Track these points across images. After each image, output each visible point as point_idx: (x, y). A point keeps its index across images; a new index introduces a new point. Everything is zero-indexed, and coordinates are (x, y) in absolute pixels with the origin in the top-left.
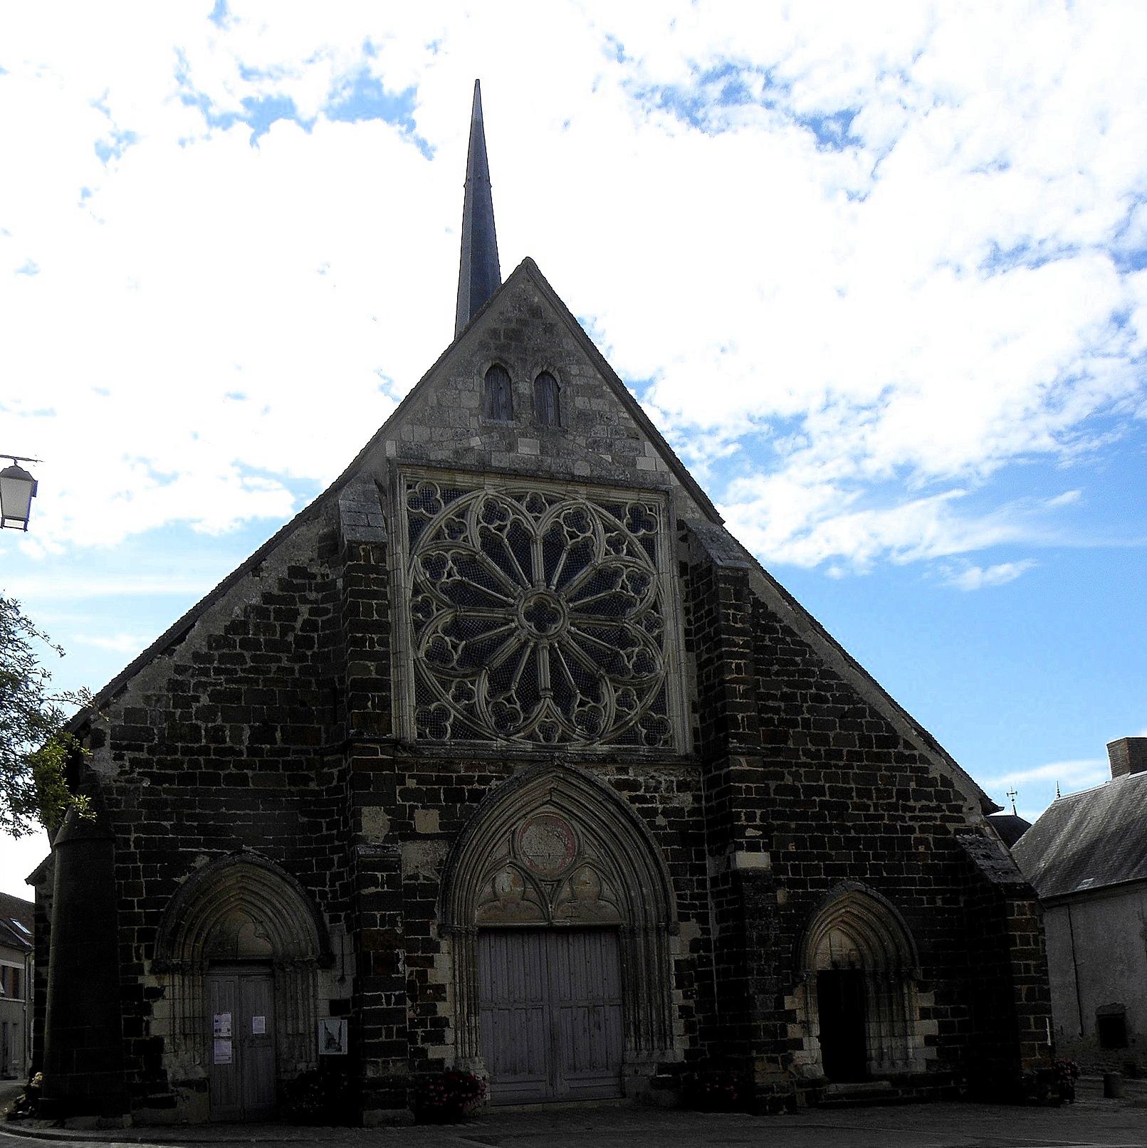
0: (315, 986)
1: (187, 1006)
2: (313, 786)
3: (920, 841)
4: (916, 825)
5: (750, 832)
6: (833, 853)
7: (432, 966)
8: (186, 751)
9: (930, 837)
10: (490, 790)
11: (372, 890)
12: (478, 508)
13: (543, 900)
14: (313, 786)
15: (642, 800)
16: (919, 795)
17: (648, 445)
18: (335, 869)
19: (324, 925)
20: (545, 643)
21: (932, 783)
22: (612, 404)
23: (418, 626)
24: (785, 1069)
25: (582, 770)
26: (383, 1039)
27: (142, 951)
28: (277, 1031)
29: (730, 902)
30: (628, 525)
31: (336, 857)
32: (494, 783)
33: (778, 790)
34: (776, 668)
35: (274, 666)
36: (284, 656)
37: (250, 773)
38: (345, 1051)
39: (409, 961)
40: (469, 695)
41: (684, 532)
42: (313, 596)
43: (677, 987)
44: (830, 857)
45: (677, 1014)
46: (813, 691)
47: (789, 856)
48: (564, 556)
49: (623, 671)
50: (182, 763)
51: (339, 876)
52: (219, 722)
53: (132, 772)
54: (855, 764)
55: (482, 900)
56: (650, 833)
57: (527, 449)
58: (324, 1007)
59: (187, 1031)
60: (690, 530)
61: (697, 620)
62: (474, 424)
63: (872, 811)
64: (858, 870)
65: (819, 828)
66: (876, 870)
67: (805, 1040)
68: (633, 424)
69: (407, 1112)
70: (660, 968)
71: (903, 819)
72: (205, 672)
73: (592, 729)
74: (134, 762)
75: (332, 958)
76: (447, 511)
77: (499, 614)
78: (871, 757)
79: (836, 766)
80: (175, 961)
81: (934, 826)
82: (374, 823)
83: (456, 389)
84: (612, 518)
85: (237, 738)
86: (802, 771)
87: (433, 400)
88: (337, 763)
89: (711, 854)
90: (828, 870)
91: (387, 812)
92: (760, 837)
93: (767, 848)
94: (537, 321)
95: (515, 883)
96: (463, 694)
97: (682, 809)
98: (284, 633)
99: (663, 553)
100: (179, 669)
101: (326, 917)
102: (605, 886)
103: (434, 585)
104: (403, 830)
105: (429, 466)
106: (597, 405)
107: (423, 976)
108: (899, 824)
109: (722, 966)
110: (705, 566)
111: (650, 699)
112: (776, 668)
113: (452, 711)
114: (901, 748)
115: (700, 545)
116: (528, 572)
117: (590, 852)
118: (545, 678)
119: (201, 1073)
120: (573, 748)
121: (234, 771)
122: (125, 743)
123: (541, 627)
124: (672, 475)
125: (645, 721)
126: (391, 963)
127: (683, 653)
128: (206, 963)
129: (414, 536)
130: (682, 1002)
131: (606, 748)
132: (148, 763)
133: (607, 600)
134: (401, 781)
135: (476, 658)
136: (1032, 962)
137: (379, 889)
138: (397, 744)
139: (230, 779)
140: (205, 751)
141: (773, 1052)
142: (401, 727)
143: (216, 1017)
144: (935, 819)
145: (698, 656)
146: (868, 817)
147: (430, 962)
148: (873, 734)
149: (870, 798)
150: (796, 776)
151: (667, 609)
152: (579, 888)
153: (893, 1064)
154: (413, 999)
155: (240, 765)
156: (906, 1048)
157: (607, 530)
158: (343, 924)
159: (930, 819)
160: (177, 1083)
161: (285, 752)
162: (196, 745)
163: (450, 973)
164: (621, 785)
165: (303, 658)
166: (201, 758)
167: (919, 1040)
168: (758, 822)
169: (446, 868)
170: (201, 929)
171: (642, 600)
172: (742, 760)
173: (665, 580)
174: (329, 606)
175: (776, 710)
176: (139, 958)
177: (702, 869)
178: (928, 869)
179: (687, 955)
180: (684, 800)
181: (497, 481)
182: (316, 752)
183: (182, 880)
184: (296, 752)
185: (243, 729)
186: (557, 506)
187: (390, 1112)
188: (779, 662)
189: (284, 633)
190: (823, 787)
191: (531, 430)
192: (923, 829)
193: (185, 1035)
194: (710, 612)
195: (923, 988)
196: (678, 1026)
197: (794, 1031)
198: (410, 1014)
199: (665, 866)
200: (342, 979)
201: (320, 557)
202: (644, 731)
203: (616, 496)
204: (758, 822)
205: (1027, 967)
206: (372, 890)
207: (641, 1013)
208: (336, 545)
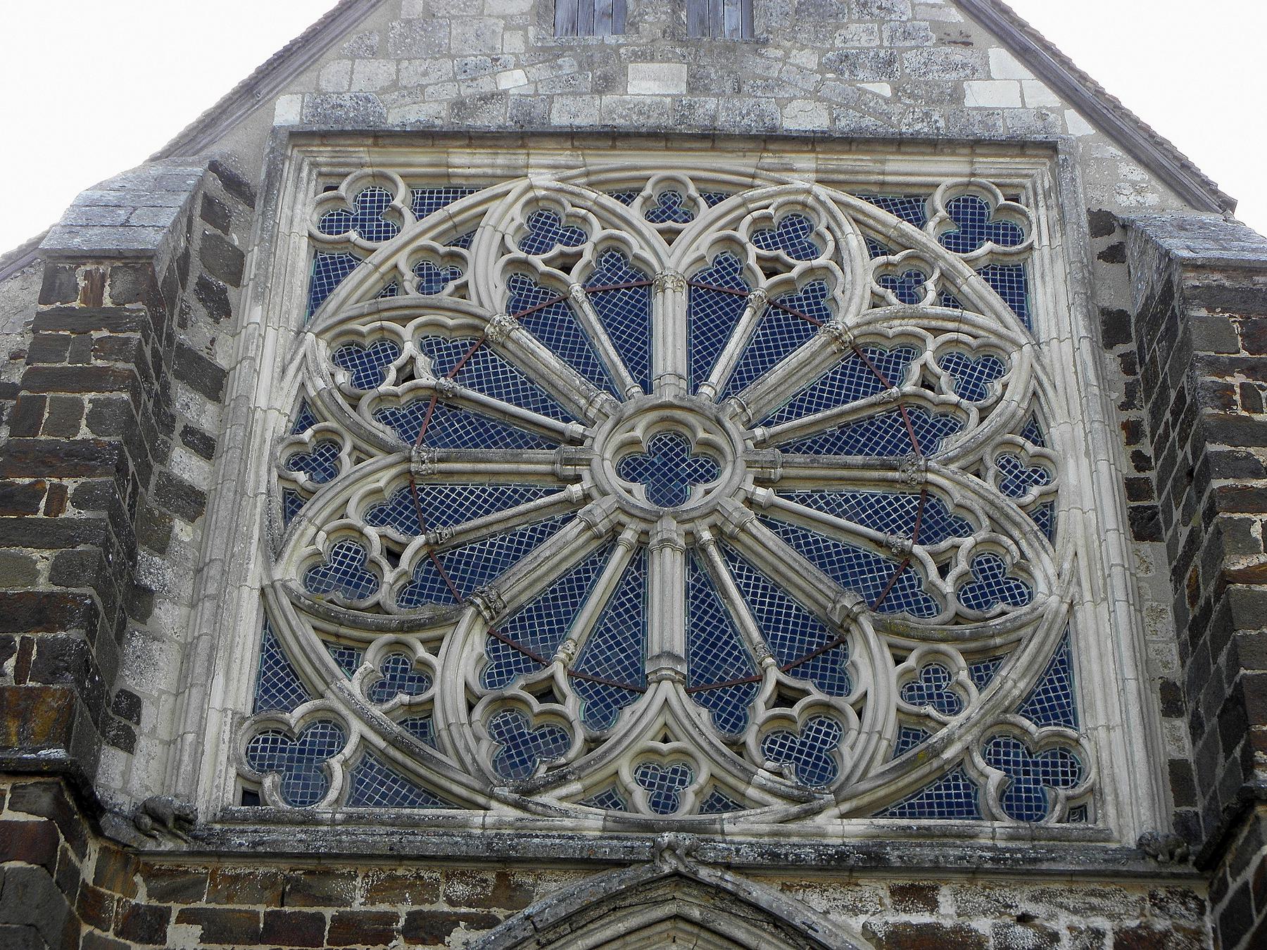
12: (504, 218)
17: (1000, 57)
25: (762, 893)
40: (423, 677)
41: (1114, 239)
49: (926, 604)
57: (652, 86)
62: (514, 43)
73: (811, 759)
77: (538, 461)
96: (406, 675)
103: (354, 402)
105: (380, 136)
111: (1014, 679)
113: (357, 727)
116: (638, 357)
118: (668, 624)
124: (1072, 115)
125: (999, 747)
131: (858, 826)
133: (873, 414)
135: (449, 580)
157: (875, 249)
171: (984, 413)
173: (1056, 352)
181: (564, 157)
191: (665, 45)
202: (996, 775)
203: (903, 169)
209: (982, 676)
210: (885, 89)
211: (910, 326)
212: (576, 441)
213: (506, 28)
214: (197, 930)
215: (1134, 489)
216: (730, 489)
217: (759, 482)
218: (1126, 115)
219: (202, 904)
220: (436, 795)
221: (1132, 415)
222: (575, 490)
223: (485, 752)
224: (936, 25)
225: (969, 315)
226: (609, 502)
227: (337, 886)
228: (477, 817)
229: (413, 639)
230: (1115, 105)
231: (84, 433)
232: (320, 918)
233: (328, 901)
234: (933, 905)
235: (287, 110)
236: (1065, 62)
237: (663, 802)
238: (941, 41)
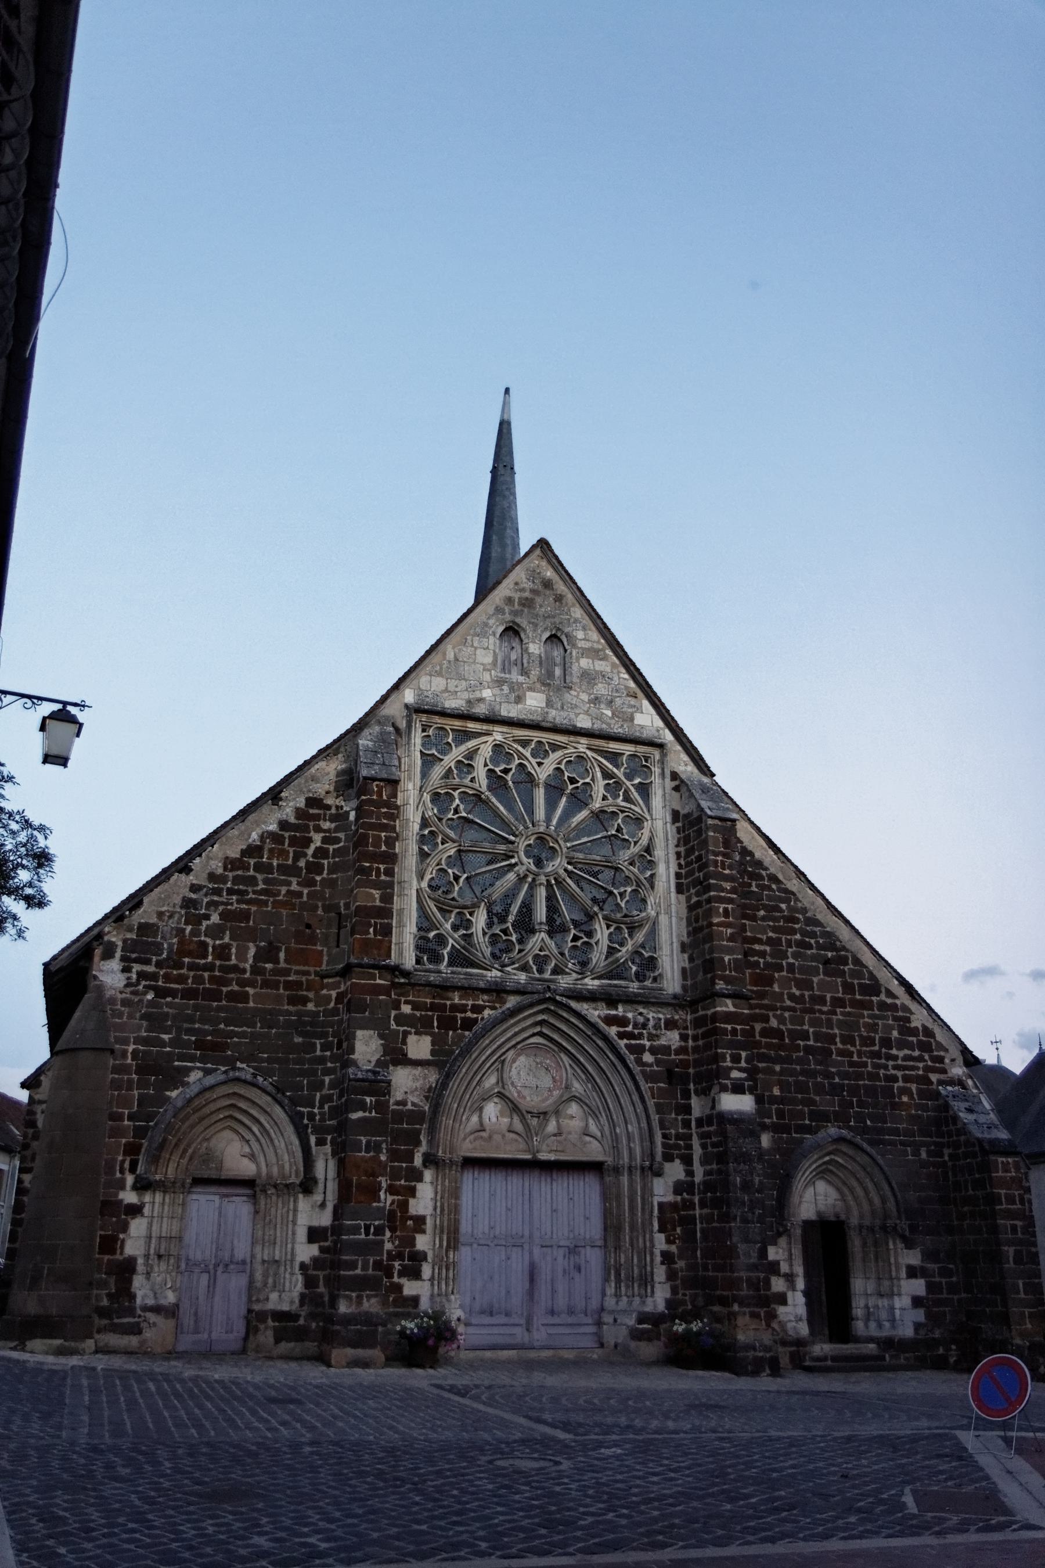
0: (295, 1210)
1: (165, 1226)
2: (311, 1006)
3: (904, 1091)
4: (899, 1074)
5: (735, 1074)
6: (818, 1098)
7: (414, 1196)
8: (192, 967)
9: (914, 1087)
10: (482, 1019)
11: (360, 1114)
12: (486, 752)
13: (529, 1132)
14: (311, 1006)
15: (630, 1036)
16: (902, 1045)
17: (646, 703)
18: (325, 1092)
20: (543, 879)
21: (914, 1032)
22: (614, 665)
23: (423, 855)
24: (768, 1325)
25: (573, 1004)
26: (358, 1271)
27: (127, 1165)
28: (253, 1256)
29: (714, 1145)
30: (625, 774)
31: (327, 1079)
32: (487, 1012)
33: (765, 1033)
34: (762, 913)
35: (284, 890)
36: (294, 881)
37: (251, 991)
39: (392, 1190)
41: (677, 783)
42: (326, 825)
43: (660, 1231)
44: (813, 1102)
45: (658, 1259)
46: (798, 937)
47: (773, 1100)
48: (564, 799)
50: (188, 978)
52: (227, 940)
53: (138, 983)
54: (838, 1010)
55: (468, 1130)
56: (637, 1069)
57: (534, 702)
58: (302, 1234)
59: (162, 1252)
60: (682, 781)
61: (688, 864)
62: (487, 677)
63: (855, 1058)
64: (841, 1118)
65: (803, 1072)
66: (860, 1118)
67: (790, 1294)
68: (632, 684)
69: (376, 1354)
70: (643, 1209)
71: (886, 1067)
72: (217, 892)
74: (141, 975)
75: (315, 1181)
76: (457, 753)
77: (502, 848)
78: (855, 1004)
79: (821, 1012)
80: (158, 1177)
81: (918, 1076)
82: (367, 1048)
83: (472, 646)
84: (610, 766)
85: (242, 956)
86: (787, 1014)
87: (450, 655)
88: (336, 986)
89: (697, 1093)
90: (815, 1116)
91: (381, 1036)
92: (745, 1079)
93: (752, 1091)
94: (548, 592)
95: (502, 1114)
97: (670, 1047)
98: (296, 858)
99: (657, 801)
100: (194, 888)
101: (313, 1139)
102: (591, 1121)
103: (440, 820)
104: (395, 1055)
105: (443, 714)
106: (601, 666)
107: (404, 1206)
108: (882, 1071)
109: (705, 1211)
110: (695, 815)
112: (762, 913)
113: (451, 941)
114: (883, 997)
115: (692, 795)
116: (531, 812)
117: (577, 1087)
118: (541, 913)
119: (171, 1298)
120: (564, 982)
121: (236, 988)
122: (134, 956)
123: (539, 863)
124: (667, 731)
126: (373, 1192)
127: (673, 895)
129: (424, 775)
130: (664, 1247)
131: (597, 982)
132: (154, 977)
134: (397, 1007)
136: (1019, 1223)
137: (367, 1114)
138: (396, 970)
139: (233, 996)
140: (210, 967)
141: (757, 1305)
142: (401, 953)
144: (918, 1068)
145: (688, 899)
146: (852, 1064)
147: (412, 1192)
148: (856, 982)
149: (854, 1045)
150: (781, 1020)
151: (659, 853)
152: (565, 1122)
153: (880, 1326)
154: (393, 1230)
155: (242, 983)
156: (892, 1308)
158: (328, 1149)
159: (913, 1068)
160: (146, 1309)
161: (287, 972)
162: (203, 961)
163: (430, 1205)
164: (610, 1021)
165: (311, 883)
166: (206, 975)
167: (905, 1301)
168: (743, 1064)
169: (435, 1096)
170: (189, 1145)
171: (636, 843)
172: (729, 1002)
173: (659, 825)
174: (341, 835)
175: (762, 954)
176: (122, 1172)
177: (687, 1109)
178: (914, 1119)
179: (670, 1198)
180: (672, 1038)
181: (505, 729)
182: (316, 974)
183: (174, 1094)
184: (297, 972)
185: (248, 948)
186: (559, 754)
187: (360, 1353)
188: (765, 907)
189: (296, 858)
190: (807, 1031)
191: (538, 685)
192: (906, 1079)
193: (160, 1257)
194: (699, 858)
195: (909, 1245)
196: (660, 1273)
197: (778, 1285)
198: (388, 1246)
199: (651, 1103)
200: (323, 1205)
201: (336, 789)
204: (743, 1064)
205: (1014, 1228)
206: (360, 1114)
207: (622, 1256)
208: (352, 779)
209: (631, 935)
210: (609, 713)
211: (614, 809)
212: (513, 843)
213: (484, 670)
214: (410, 1007)
215: (678, 876)
216: (557, 865)
217: (568, 863)
218: (685, 736)
219: (410, 998)
220: (473, 965)
221: (679, 849)
222: (513, 861)
223: (488, 952)
224: (627, 688)
225: (633, 807)
226: (524, 868)
227: (450, 994)
228: (489, 974)
229: (466, 911)
230: (681, 730)
231: (384, 848)
232: (445, 1004)
233: (448, 999)
234: (617, 1009)
235: (409, 696)
236: (668, 711)
237: (541, 971)
238: (628, 695)
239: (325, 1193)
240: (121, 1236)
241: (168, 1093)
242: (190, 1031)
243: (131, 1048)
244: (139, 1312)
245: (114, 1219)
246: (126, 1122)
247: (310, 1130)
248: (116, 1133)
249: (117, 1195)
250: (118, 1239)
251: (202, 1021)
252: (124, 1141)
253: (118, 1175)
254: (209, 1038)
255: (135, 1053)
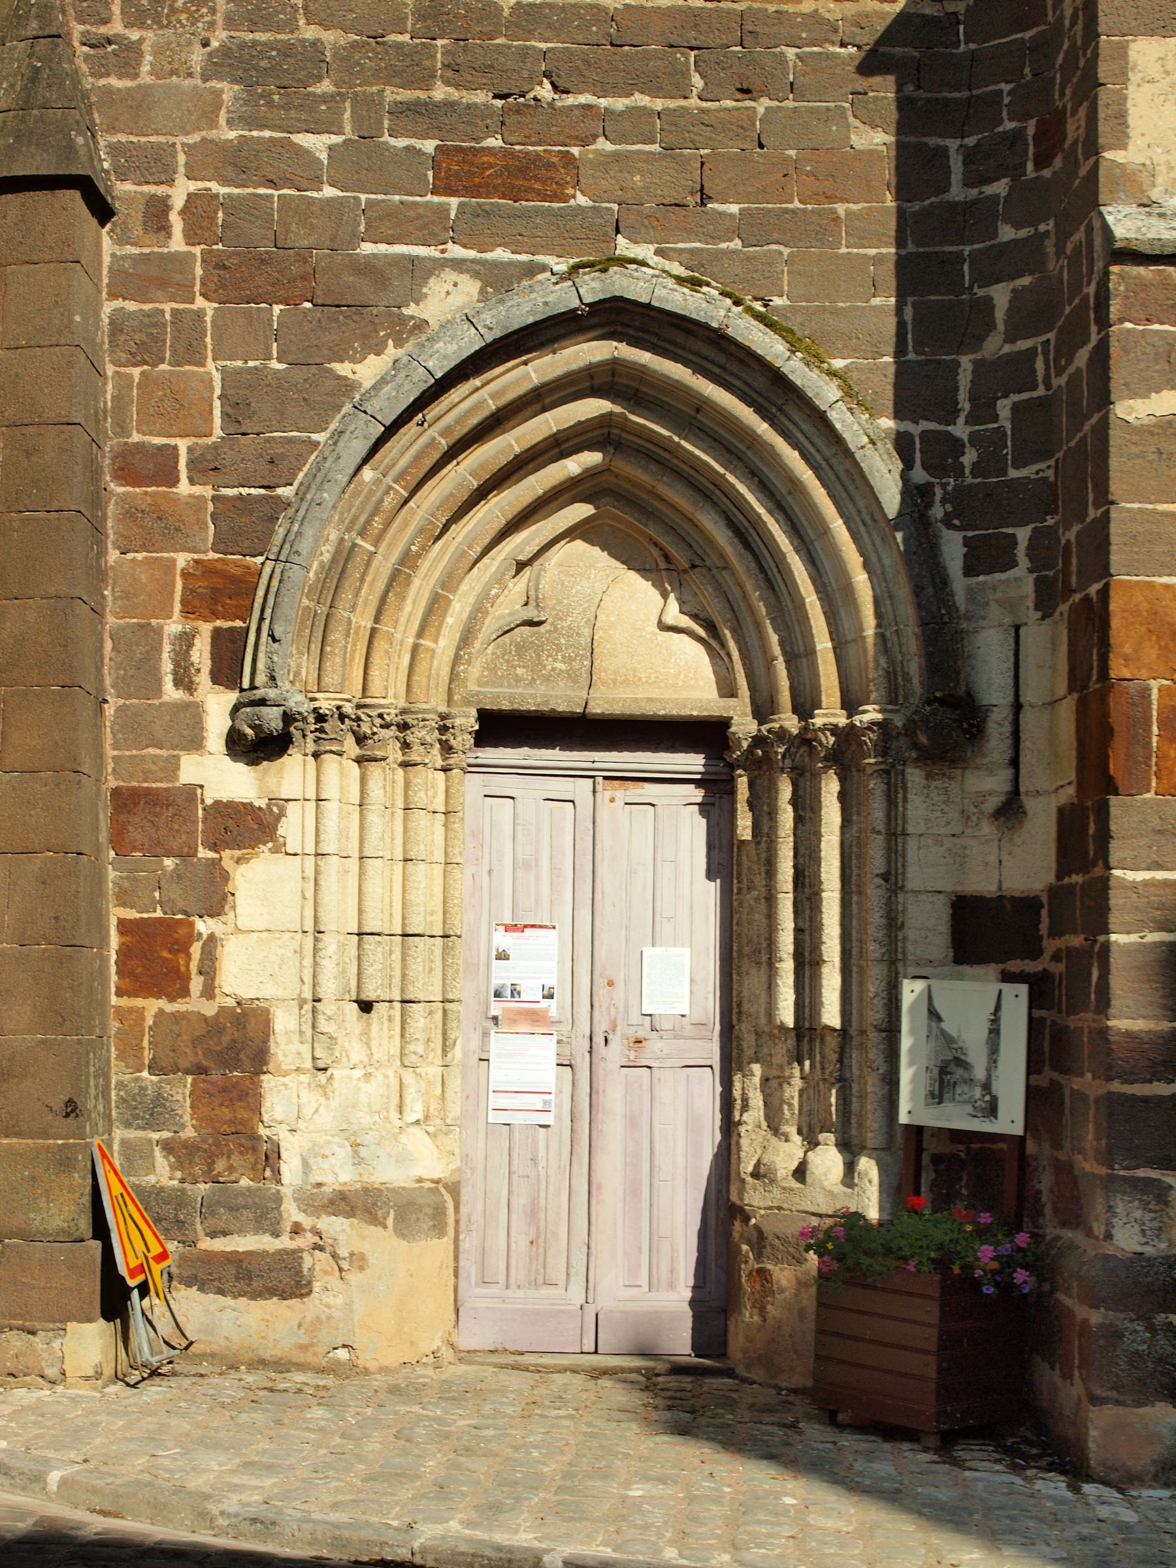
18: (995, 345)
19: (941, 581)
27: (201, 654)
31: (1001, 295)
38: (1011, 1119)
51: (1017, 371)
101: (953, 548)
128: (468, 721)
143: (502, 940)
158: (1020, 580)
176: (184, 680)
183: (366, 371)
193: (366, 1007)
200: (1010, 810)
239: (1015, 763)
240: (203, 926)
241: (343, 369)
242: (415, 116)
243: (180, 191)
244: (292, 1213)
245: (169, 863)
246: (184, 488)
247: (938, 511)
248: (158, 528)
249: (173, 767)
250: (192, 936)
251: (455, 72)
252: (182, 559)
253: (171, 692)
254: (494, 142)
255: (198, 210)
